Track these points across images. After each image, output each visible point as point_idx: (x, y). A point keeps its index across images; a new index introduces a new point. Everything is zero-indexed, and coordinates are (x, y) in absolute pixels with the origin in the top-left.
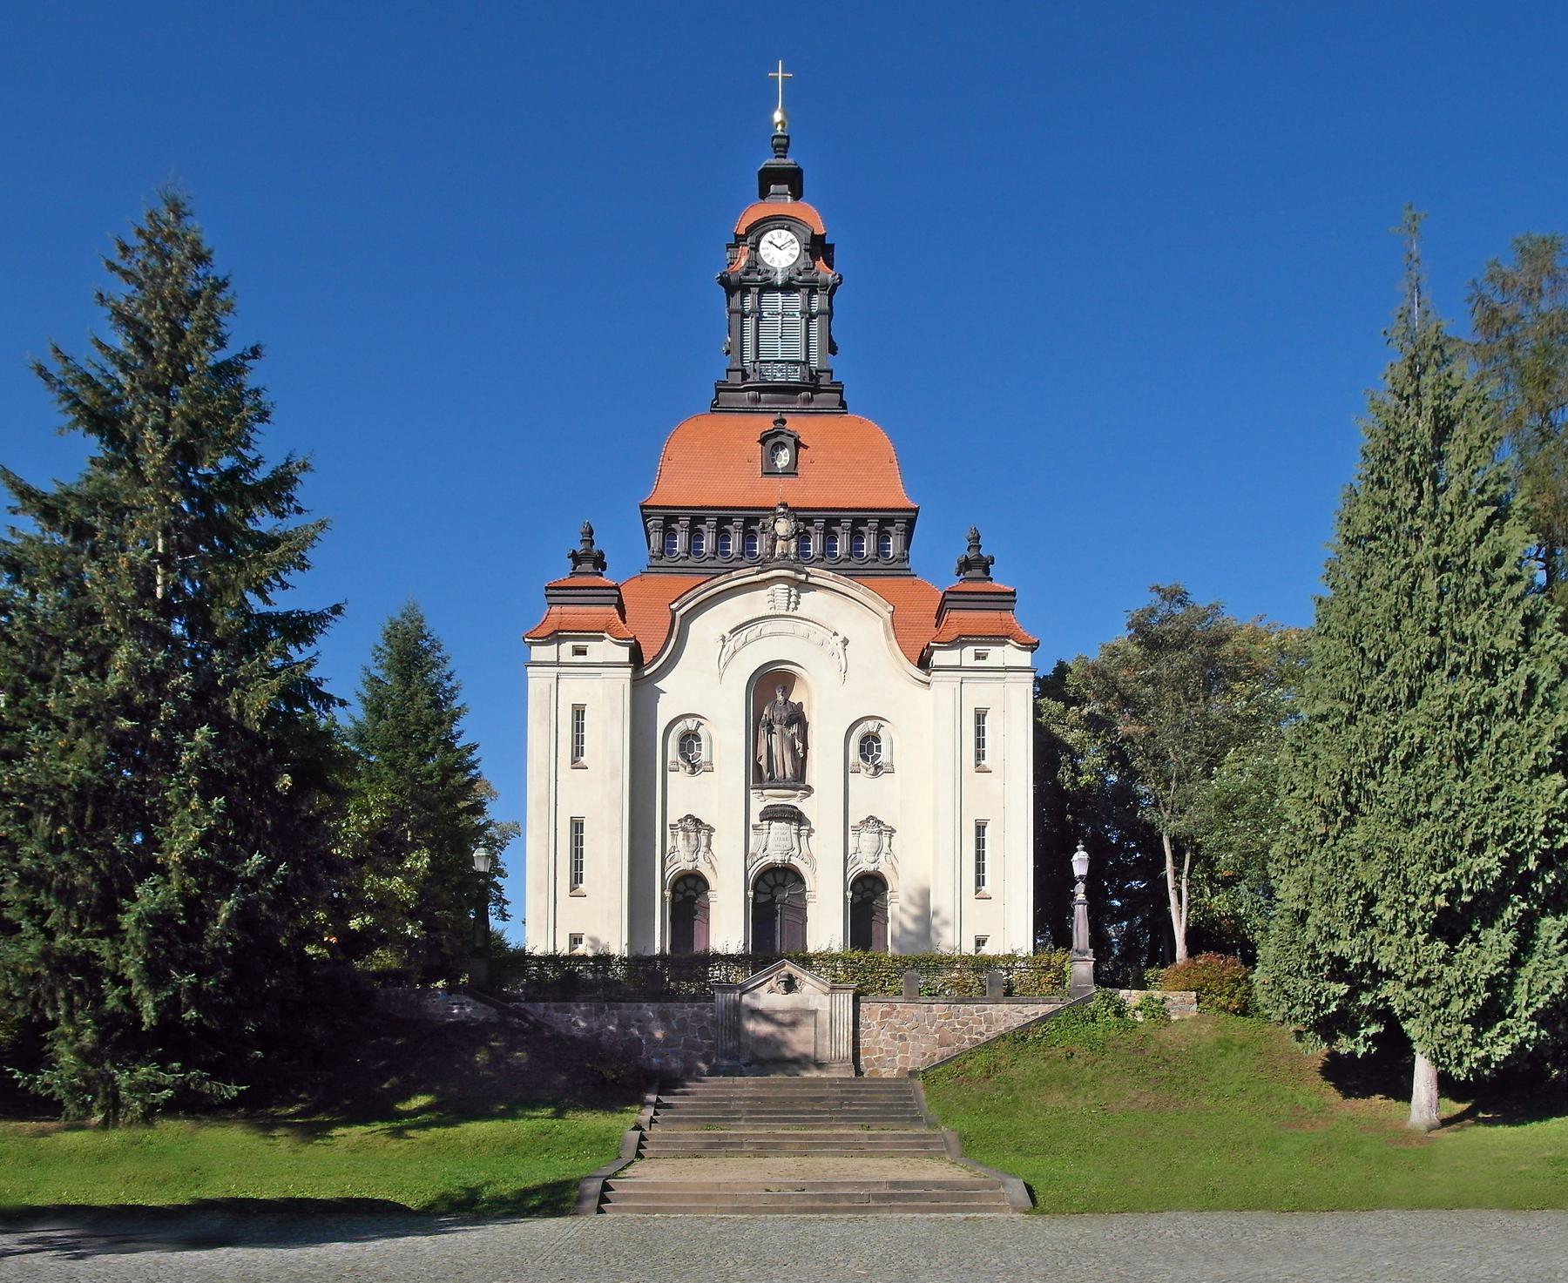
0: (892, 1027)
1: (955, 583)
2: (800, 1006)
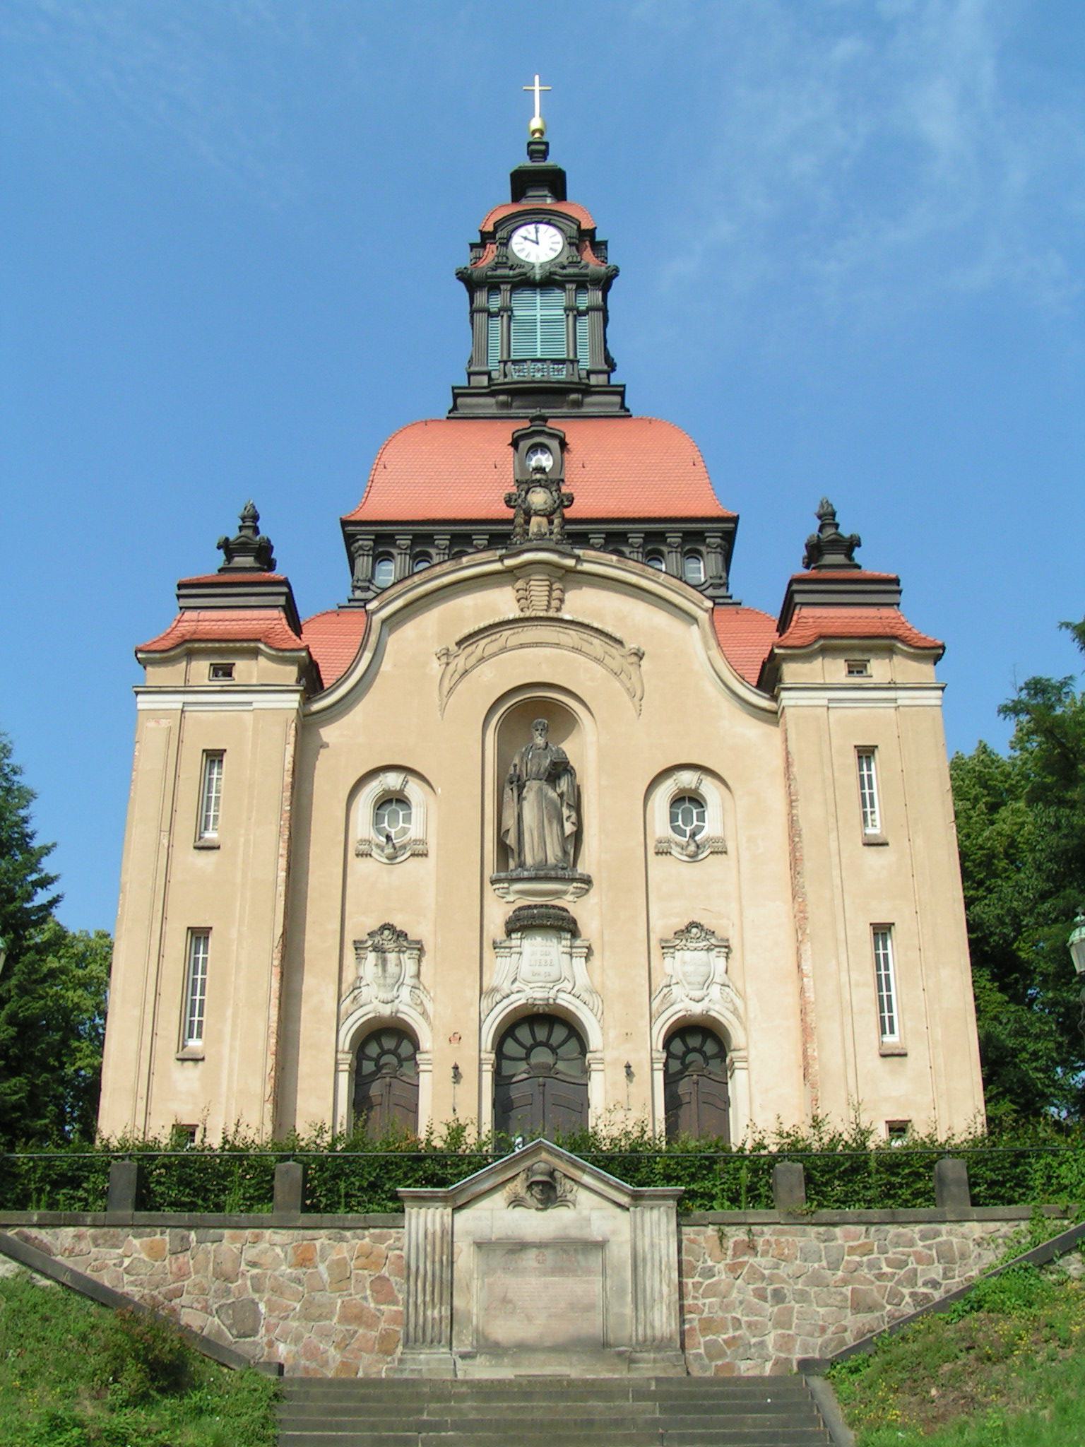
0: (756, 1274)
1: (802, 572)
2: (574, 1233)
